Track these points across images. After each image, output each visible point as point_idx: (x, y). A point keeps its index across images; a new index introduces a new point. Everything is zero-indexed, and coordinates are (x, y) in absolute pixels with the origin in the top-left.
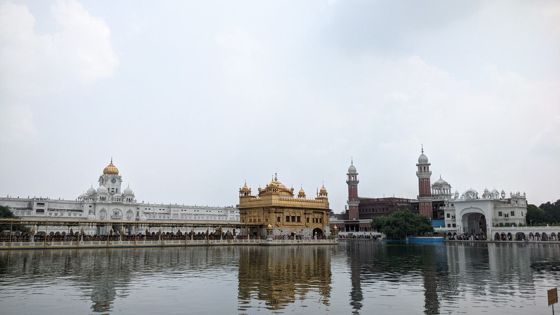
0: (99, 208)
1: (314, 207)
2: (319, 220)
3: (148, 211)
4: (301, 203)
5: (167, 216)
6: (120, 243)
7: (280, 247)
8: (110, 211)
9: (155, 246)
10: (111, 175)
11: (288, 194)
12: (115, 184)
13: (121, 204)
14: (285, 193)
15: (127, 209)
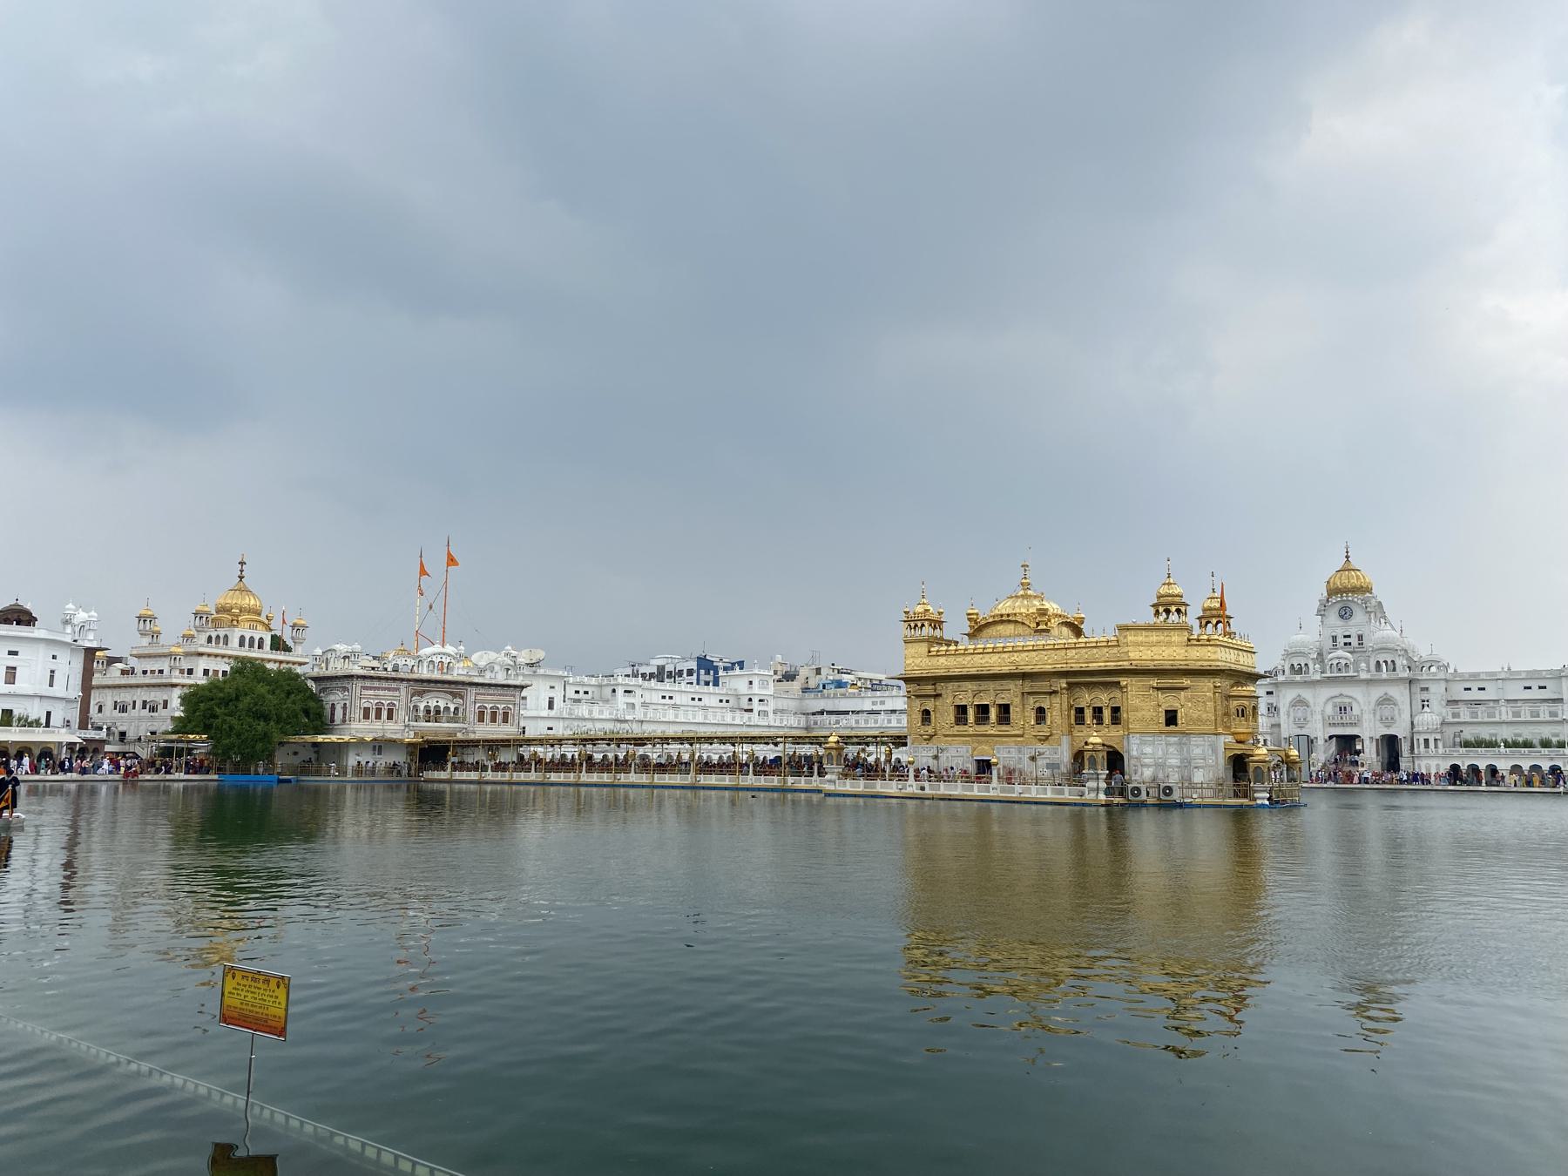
0: (1285, 698)
1: (1066, 668)
2: (1107, 714)
3: (1475, 695)
4: (1015, 657)
5: (1544, 712)
6: (633, 778)
7: (861, 801)
8: (1321, 701)
9: (683, 787)
10: (1346, 596)
11: (1020, 629)
12: (1353, 621)
13: (1352, 681)
14: (1010, 628)
15: (1377, 693)
